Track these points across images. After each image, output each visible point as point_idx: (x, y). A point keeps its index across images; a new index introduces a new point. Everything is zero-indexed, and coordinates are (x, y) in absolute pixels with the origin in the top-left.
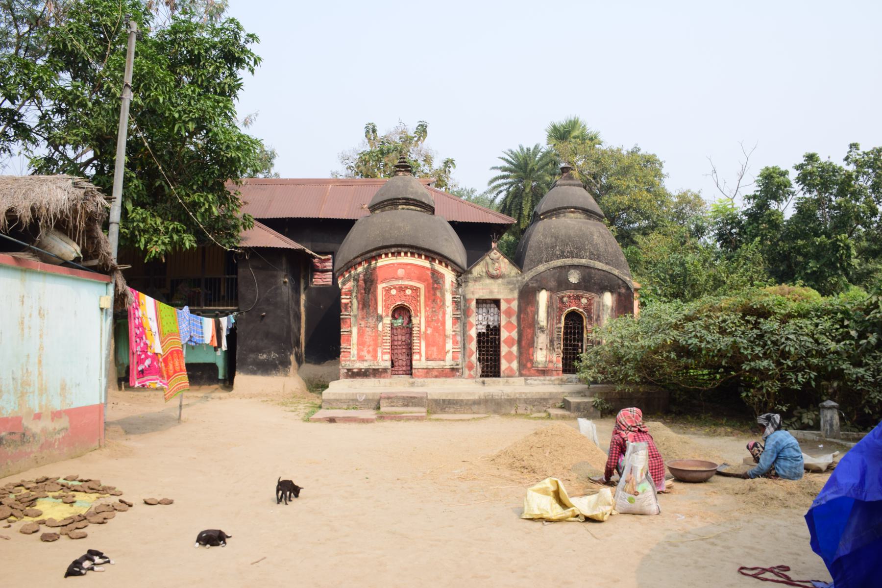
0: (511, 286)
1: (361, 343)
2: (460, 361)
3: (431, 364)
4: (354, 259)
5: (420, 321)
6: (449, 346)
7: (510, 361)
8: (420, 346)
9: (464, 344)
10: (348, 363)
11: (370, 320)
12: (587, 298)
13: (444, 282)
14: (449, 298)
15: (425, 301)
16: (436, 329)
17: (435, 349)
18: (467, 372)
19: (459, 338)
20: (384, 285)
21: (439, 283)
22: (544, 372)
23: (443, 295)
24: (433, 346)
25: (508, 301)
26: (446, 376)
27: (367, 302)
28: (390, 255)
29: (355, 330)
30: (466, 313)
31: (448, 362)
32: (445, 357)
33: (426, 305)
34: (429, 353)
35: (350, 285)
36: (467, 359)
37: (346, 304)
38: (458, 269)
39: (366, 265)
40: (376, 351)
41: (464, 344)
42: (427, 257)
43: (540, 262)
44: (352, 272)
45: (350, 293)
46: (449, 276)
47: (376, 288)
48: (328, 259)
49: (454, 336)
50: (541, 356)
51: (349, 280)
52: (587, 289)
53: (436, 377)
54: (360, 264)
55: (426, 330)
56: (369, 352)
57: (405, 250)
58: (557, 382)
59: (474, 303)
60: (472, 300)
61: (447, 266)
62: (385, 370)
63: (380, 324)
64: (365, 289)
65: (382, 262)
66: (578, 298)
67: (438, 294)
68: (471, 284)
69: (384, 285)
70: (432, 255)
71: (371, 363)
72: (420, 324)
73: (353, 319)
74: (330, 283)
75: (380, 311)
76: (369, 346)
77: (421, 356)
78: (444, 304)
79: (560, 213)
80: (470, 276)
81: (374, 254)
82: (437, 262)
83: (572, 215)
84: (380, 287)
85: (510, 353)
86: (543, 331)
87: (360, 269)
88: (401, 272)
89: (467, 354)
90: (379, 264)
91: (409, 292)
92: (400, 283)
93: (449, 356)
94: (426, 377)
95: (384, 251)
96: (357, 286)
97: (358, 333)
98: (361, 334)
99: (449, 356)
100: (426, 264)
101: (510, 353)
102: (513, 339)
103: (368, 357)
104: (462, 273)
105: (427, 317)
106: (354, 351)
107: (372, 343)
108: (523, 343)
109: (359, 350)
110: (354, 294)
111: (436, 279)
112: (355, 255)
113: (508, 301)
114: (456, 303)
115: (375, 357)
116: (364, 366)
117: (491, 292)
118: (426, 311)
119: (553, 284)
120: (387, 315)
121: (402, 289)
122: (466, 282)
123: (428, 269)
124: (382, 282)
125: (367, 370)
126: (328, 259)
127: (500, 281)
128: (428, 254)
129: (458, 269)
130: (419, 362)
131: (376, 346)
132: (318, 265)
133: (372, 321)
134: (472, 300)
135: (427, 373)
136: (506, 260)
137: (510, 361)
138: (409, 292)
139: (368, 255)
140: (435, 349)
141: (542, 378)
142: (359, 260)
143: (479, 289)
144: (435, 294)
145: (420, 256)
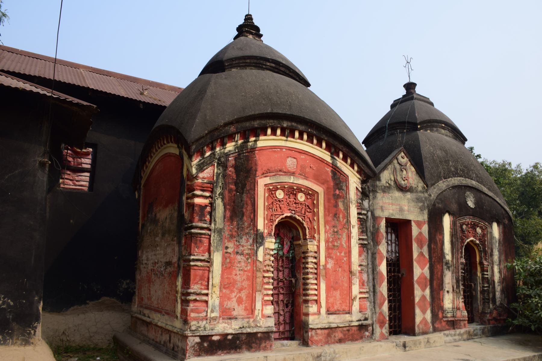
0: (421, 204)
1: (227, 285)
2: (368, 313)
3: (335, 320)
4: (226, 125)
5: (317, 246)
6: (356, 290)
7: (424, 312)
8: (319, 290)
9: (374, 286)
10: (203, 323)
11: (243, 241)
12: (481, 228)
13: (347, 187)
14: (354, 211)
15: (325, 215)
16: (338, 262)
17: (337, 294)
18: (378, 330)
19: (365, 277)
20: (267, 180)
21: (340, 189)
22: (453, 324)
23: (347, 208)
24: (335, 289)
25: (419, 224)
26: (353, 339)
27: (240, 208)
28: (279, 132)
29: (217, 258)
30: (375, 238)
31: (355, 317)
32: (351, 306)
33: (326, 222)
34: (331, 300)
35: (208, 173)
36: (377, 310)
37: (202, 208)
38: (367, 170)
39: (240, 142)
40: (253, 301)
41: (374, 286)
42: (328, 148)
43: (439, 178)
44: (218, 149)
45: (211, 186)
46: (354, 181)
47: (254, 184)
48: (87, 154)
49: (360, 272)
50: (449, 301)
51: (211, 164)
52: (483, 218)
53: (340, 341)
54: (231, 137)
55: (326, 262)
56: (240, 301)
57: (302, 128)
58: (465, 336)
59: (383, 223)
60: (382, 218)
61: (352, 166)
62: (267, 335)
63: (261, 249)
64: (236, 184)
65: (264, 142)
66: (474, 226)
67: (341, 205)
68: (379, 195)
69: (267, 180)
70: (336, 143)
71: (245, 323)
72: (318, 252)
73: (214, 237)
74: (86, 189)
75: (261, 226)
76: (240, 290)
77: (320, 307)
78: (349, 222)
79: (433, 126)
80: (378, 183)
81: (256, 124)
82: (341, 156)
83: (443, 131)
84: (262, 182)
85: (423, 297)
86: (448, 268)
87: (230, 147)
88: (291, 163)
89: (378, 302)
90: (260, 144)
91: (301, 197)
92: (292, 180)
93: (356, 306)
94: (327, 343)
95: (271, 122)
96: (224, 176)
97: (223, 264)
98: (227, 266)
99: (356, 306)
100: (326, 156)
101: (423, 297)
102: (426, 278)
103: (239, 311)
104: (369, 177)
105: (327, 241)
106: (214, 300)
107: (246, 284)
108: (435, 282)
109: (223, 298)
110: (218, 191)
111: (339, 179)
112: (227, 119)
113: (419, 224)
114: (362, 222)
115: (252, 311)
116: (230, 328)
117: (401, 210)
118: (325, 232)
119: (454, 207)
120: (269, 234)
121: (292, 191)
122: (374, 191)
123: (327, 164)
124: (265, 174)
125: (236, 336)
126: (87, 154)
127: (409, 195)
128: (331, 141)
129: (367, 170)
130: (317, 317)
131: (253, 290)
132: (70, 159)
133: (246, 243)
134: (382, 218)
135: (329, 335)
136: (413, 169)
137: (424, 312)
138: (301, 197)
139: (248, 124)
140: (337, 294)
141: (452, 332)
142: (232, 129)
143: (393, 205)
144: (336, 206)
145: (320, 144)
